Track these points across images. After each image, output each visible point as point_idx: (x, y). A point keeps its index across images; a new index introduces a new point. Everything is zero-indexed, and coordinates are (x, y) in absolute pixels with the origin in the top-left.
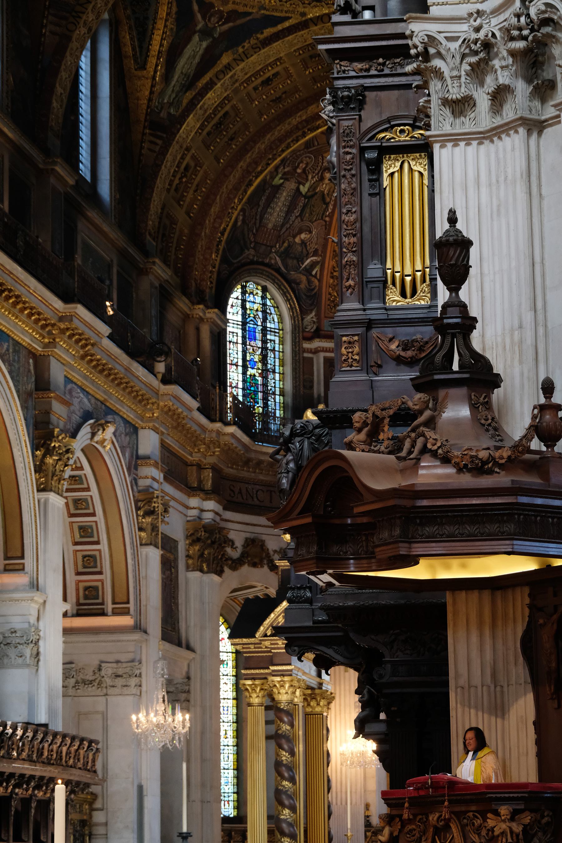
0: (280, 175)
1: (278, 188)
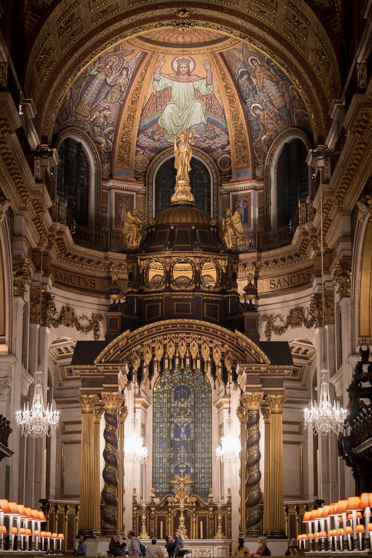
0: (96, 68)
1: (94, 76)
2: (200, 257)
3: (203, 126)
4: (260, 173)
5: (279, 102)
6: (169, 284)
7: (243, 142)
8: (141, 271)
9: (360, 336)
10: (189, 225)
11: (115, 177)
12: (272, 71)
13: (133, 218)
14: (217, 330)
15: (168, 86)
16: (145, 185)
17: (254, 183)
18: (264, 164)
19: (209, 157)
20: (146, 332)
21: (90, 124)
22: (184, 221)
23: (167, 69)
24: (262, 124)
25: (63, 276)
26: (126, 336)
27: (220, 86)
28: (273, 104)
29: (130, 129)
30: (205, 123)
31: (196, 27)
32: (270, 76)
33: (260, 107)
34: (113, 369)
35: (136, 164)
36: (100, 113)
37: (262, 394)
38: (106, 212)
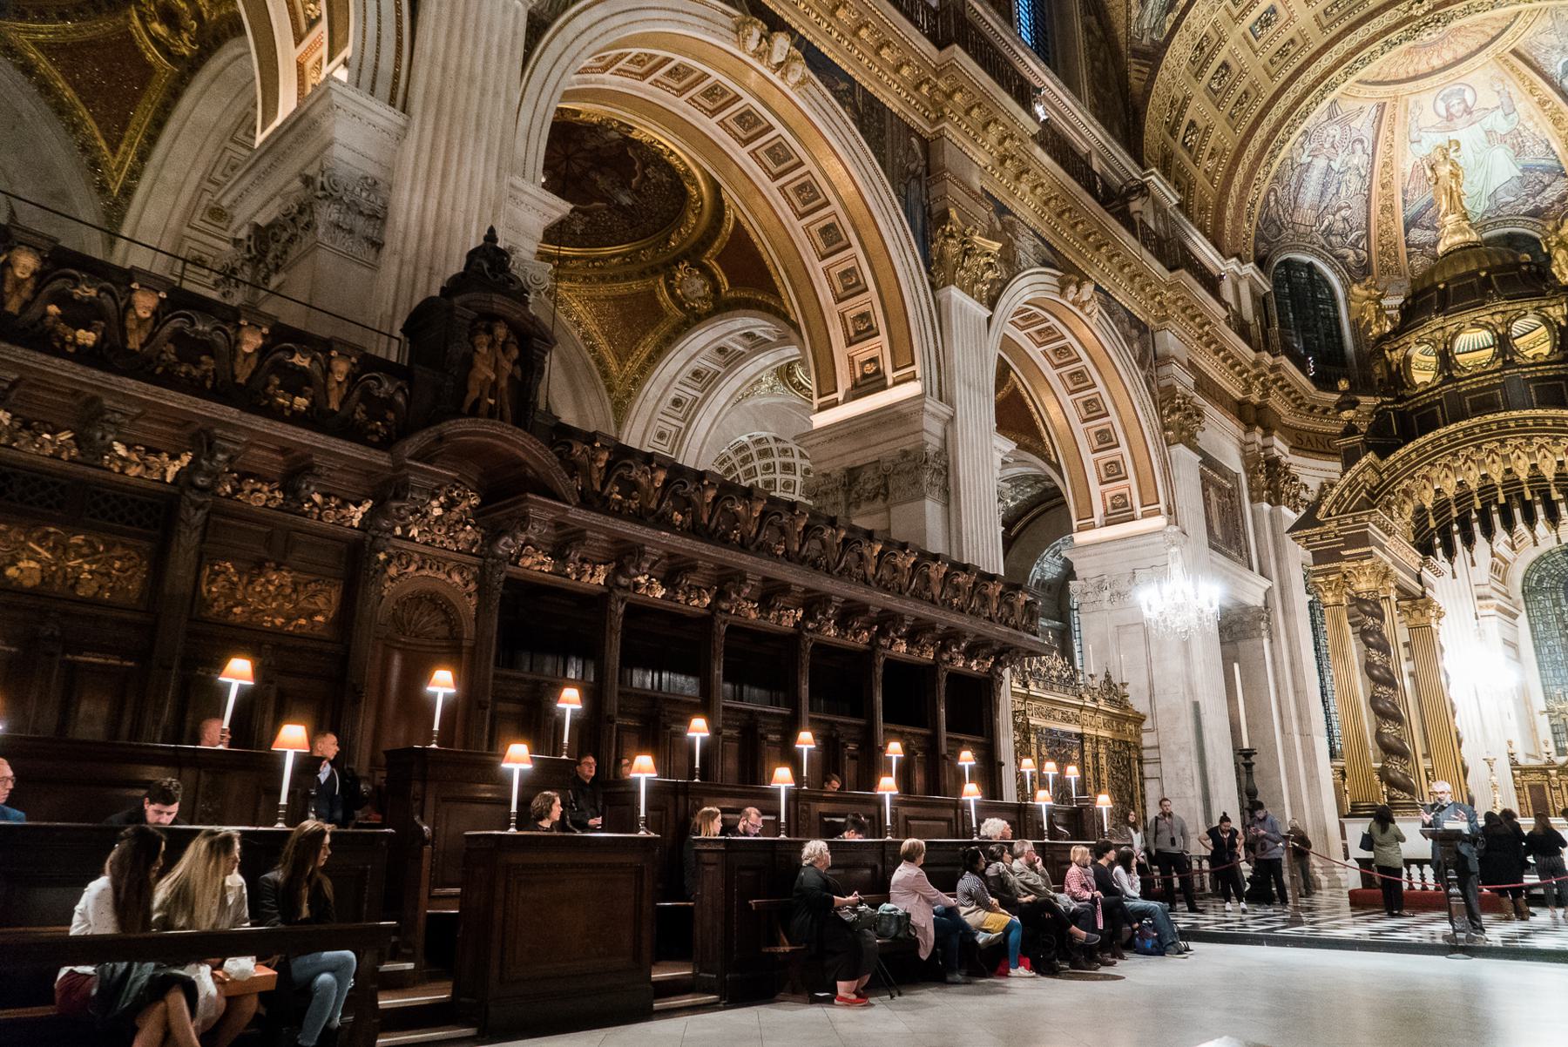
0: (1307, 153)
2: (1503, 312)
3: (1515, 181)
10: (1475, 274)
13: (1365, 293)
20: (1413, 456)
22: (1463, 270)
23: (1428, 117)
25: (1314, 441)
29: (1391, 223)
31: (1453, 25)
34: (1355, 522)
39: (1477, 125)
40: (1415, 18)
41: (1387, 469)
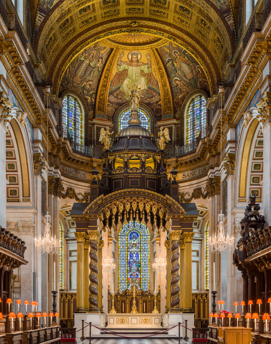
4: (178, 116)
5: (190, 76)
6: (127, 169)
7: (168, 99)
8: (110, 162)
9: (240, 197)
11: (96, 118)
12: (186, 58)
14: (155, 195)
15: (126, 68)
16: (113, 123)
17: (175, 121)
18: (180, 111)
19: (149, 108)
21: (81, 89)
24: (179, 88)
26: (102, 198)
27: (155, 68)
28: (186, 77)
30: (147, 89)
32: (185, 61)
33: (179, 79)
34: (94, 217)
35: (108, 111)
36: (87, 82)
37: (181, 231)
38: (91, 137)
39: (139, 67)
40: (132, 27)
41: (105, 199)
